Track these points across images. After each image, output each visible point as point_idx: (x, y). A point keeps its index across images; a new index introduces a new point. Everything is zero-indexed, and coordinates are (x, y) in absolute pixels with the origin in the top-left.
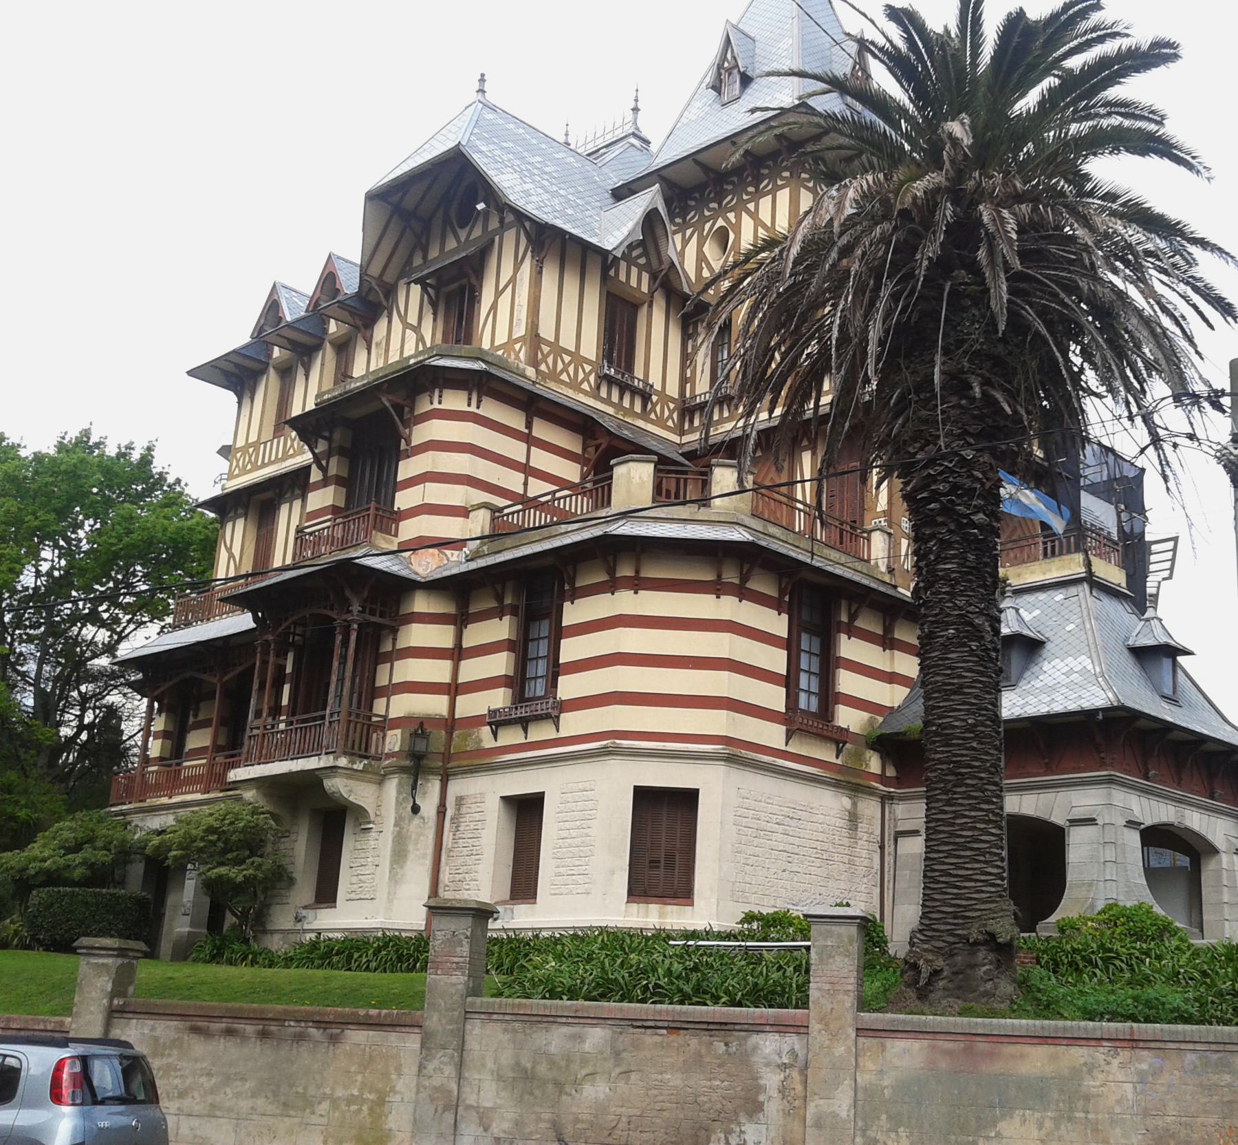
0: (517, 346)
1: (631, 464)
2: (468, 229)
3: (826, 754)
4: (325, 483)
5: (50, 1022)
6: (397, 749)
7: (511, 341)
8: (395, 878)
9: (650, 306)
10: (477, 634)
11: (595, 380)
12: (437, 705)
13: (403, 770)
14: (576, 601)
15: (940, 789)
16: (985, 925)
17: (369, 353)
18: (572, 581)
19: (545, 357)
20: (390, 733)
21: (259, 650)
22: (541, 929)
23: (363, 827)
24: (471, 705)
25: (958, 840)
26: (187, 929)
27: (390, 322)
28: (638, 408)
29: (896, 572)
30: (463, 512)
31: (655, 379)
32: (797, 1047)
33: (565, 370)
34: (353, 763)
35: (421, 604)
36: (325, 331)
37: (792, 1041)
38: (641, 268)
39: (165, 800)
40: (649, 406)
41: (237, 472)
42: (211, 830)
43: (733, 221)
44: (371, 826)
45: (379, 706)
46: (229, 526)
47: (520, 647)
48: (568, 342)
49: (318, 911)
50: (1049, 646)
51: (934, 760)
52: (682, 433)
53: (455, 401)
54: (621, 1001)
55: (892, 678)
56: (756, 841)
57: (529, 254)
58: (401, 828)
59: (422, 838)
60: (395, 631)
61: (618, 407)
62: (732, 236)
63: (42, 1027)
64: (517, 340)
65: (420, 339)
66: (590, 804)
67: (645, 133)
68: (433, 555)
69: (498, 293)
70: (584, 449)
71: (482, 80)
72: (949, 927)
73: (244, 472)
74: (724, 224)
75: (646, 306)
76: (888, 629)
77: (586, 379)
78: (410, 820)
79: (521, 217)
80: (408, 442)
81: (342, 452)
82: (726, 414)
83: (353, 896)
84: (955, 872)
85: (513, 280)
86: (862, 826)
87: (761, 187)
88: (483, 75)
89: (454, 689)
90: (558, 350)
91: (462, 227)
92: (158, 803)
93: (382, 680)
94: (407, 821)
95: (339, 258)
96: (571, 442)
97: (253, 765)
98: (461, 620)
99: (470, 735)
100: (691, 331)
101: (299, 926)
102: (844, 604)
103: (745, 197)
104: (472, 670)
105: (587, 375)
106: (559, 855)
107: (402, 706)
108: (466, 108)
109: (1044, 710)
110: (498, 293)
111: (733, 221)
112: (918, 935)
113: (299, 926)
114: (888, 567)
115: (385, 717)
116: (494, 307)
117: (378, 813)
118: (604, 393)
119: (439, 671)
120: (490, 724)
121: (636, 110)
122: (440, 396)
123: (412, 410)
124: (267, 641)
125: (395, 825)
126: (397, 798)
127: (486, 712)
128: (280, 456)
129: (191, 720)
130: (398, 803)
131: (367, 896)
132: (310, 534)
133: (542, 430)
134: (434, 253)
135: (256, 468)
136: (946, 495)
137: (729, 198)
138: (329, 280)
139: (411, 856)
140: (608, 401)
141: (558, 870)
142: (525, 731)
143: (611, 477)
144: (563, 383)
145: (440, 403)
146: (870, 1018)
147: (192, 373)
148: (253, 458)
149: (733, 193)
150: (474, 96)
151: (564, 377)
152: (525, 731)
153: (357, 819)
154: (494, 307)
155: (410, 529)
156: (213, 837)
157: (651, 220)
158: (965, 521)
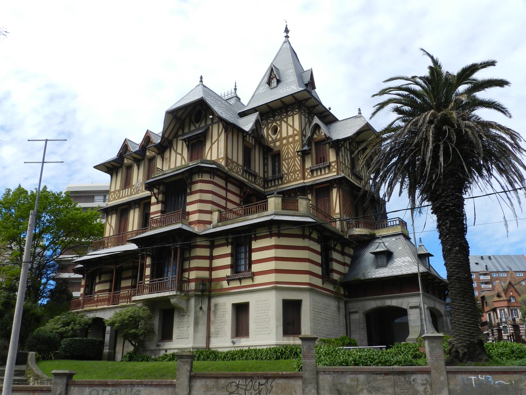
0: (221, 160)
2: (199, 123)
3: (331, 287)
4: (158, 202)
7: (218, 158)
9: (255, 149)
10: (217, 252)
11: (242, 171)
12: (205, 274)
14: (257, 241)
15: (459, 296)
16: (479, 338)
18: (255, 235)
19: (230, 164)
20: (191, 283)
25: (467, 312)
26: (108, 351)
28: (253, 181)
29: (344, 232)
30: (210, 212)
31: (257, 171)
32: (428, 378)
33: (235, 168)
34: (181, 293)
37: (425, 376)
38: (253, 137)
39: (95, 308)
40: (256, 180)
41: (117, 198)
42: (130, 317)
43: (279, 124)
44: (185, 314)
45: (186, 275)
46: (110, 217)
47: (235, 256)
48: (235, 159)
50: (394, 254)
51: (455, 287)
52: (265, 188)
53: (206, 177)
54: (384, 366)
55: (344, 264)
56: (318, 316)
57: (224, 131)
61: (248, 180)
64: (221, 159)
65: (183, 157)
67: (239, 96)
68: (202, 226)
70: (241, 192)
71: (201, 78)
72: (467, 339)
75: (254, 149)
76: (343, 249)
77: (240, 171)
79: (221, 120)
80: (191, 190)
81: (163, 193)
83: (179, 337)
84: (467, 322)
86: (341, 310)
87: (288, 114)
88: (201, 76)
89: (211, 269)
90: (233, 162)
91: (197, 122)
92: (93, 308)
93: (186, 266)
95: (150, 132)
96: (237, 191)
100: (266, 156)
101: (158, 348)
102: (332, 241)
103: (283, 117)
104: (217, 263)
105: (240, 170)
107: (193, 275)
108: (197, 86)
109: (400, 273)
110: (212, 144)
111: (279, 124)
112: (455, 342)
113: (158, 348)
114: (341, 230)
115: (188, 278)
118: (245, 176)
119: (205, 263)
120: (227, 280)
121: (235, 89)
122: (202, 176)
123: (191, 179)
124: (143, 254)
126: (195, 305)
127: (226, 276)
128: (129, 194)
129: (97, 281)
130: (195, 306)
131: (185, 337)
132: (155, 220)
133: (230, 187)
134: (186, 130)
135: (119, 198)
136: (452, 207)
137: (277, 117)
138: (147, 138)
140: (246, 178)
141: (257, 327)
142: (240, 282)
143: (267, 201)
144: (234, 172)
145: (202, 178)
146: (450, 368)
147: (95, 167)
148: (118, 195)
149: (279, 115)
151: (234, 170)
152: (240, 282)
153: (179, 312)
156: (131, 319)
157: (257, 123)
158: (458, 215)
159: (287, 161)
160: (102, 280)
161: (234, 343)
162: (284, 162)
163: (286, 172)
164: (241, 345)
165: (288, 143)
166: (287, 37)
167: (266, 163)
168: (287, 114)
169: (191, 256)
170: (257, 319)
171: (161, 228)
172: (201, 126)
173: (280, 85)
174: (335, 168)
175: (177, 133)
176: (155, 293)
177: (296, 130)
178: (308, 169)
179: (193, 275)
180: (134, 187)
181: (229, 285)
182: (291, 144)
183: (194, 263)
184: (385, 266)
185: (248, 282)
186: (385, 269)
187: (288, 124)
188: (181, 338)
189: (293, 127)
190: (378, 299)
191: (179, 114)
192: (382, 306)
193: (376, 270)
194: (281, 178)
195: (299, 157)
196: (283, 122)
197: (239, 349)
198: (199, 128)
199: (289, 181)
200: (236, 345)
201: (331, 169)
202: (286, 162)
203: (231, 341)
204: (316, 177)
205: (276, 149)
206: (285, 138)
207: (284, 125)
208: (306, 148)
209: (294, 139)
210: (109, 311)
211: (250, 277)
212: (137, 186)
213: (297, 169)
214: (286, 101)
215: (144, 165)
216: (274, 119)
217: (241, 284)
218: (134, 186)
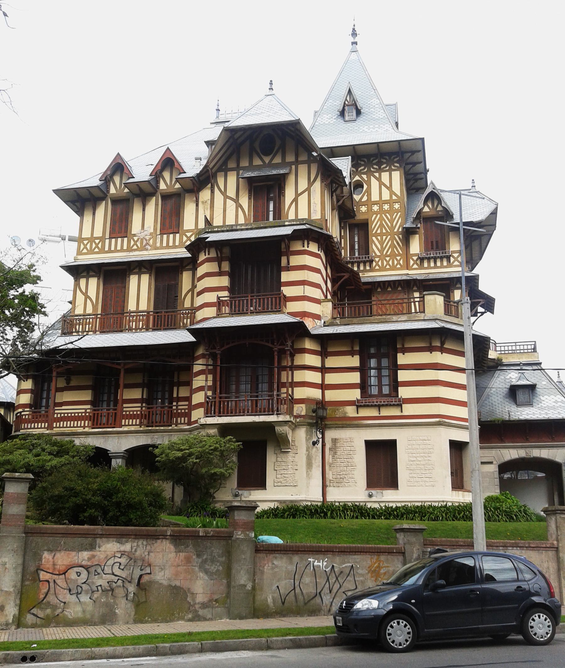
1: (436, 296)
5: (548, 544)
6: (303, 413)
8: (309, 476)
10: (331, 362)
12: (316, 394)
13: (310, 425)
17: (197, 205)
21: (219, 356)
22: (447, 502)
23: (283, 450)
24: (331, 396)
27: (212, 192)
35: (308, 344)
36: (158, 187)
43: (366, 179)
44: (289, 450)
47: (363, 369)
49: (251, 491)
53: (313, 247)
58: (309, 452)
59: (317, 457)
60: (292, 356)
62: (365, 187)
63: (544, 546)
65: (239, 206)
66: (429, 447)
69: (297, 195)
71: (271, 83)
73: (91, 252)
74: (360, 179)
78: (312, 448)
82: (368, 268)
83: (279, 484)
85: (308, 190)
88: (271, 81)
91: (267, 154)
94: (311, 448)
97: (215, 416)
98: (324, 354)
99: (337, 410)
100: (342, 225)
104: (331, 379)
106: (412, 468)
107: (300, 393)
110: (297, 195)
111: (366, 179)
116: (296, 200)
117: (293, 444)
122: (308, 244)
125: (307, 451)
126: (306, 438)
130: (307, 440)
131: (292, 484)
134: (245, 163)
135: (102, 251)
137: (362, 168)
139: (314, 466)
141: (411, 475)
145: (308, 247)
147: (56, 192)
154: (296, 200)
155: (292, 307)
159: (379, 238)
160: (72, 384)
161: (370, 496)
162: (374, 238)
163: (378, 254)
164: (385, 498)
165: (381, 211)
167: (343, 234)
169: (295, 364)
170: (411, 465)
171: (238, 316)
172: (273, 162)
173: (362, 118)
174: (458, 261)
175: (225, 163)
176: (243, 415)
177: (396, 195)
178: (415, 255)
179: (300, 393)
180: (136, 238)
181: (358, 413)
182: (387, 214)
183: (299, 376)
184: (529, 404)
185: (395, 412)
186: (531, 408)
187: (381, 184)
188: (282, 485)
189: (390, 188)
190: (522, 447)
191: (236, 136)
192: (526, 456)
193: (519, 409)
194: (371, 262)
195: (401, 236)
197: (403, 504)
198: (277, 166)
199: (383, 269)
200: (374, 499)
201: (452, 261)
202: (377, 239)
203: (367, 492)
204: (426, 268)
205: (360, 217)
206: (375, 203)
207: (374, 183)
208: (408, 225)
209: (391, 207)
210: (117, 438)
211: (398, 405)
212: (142, 237)
213: (397, 253)
214: (384, 148)
215: (157, 205)
216: (357, 170)
217: (380, 414)
218: (135, 235)
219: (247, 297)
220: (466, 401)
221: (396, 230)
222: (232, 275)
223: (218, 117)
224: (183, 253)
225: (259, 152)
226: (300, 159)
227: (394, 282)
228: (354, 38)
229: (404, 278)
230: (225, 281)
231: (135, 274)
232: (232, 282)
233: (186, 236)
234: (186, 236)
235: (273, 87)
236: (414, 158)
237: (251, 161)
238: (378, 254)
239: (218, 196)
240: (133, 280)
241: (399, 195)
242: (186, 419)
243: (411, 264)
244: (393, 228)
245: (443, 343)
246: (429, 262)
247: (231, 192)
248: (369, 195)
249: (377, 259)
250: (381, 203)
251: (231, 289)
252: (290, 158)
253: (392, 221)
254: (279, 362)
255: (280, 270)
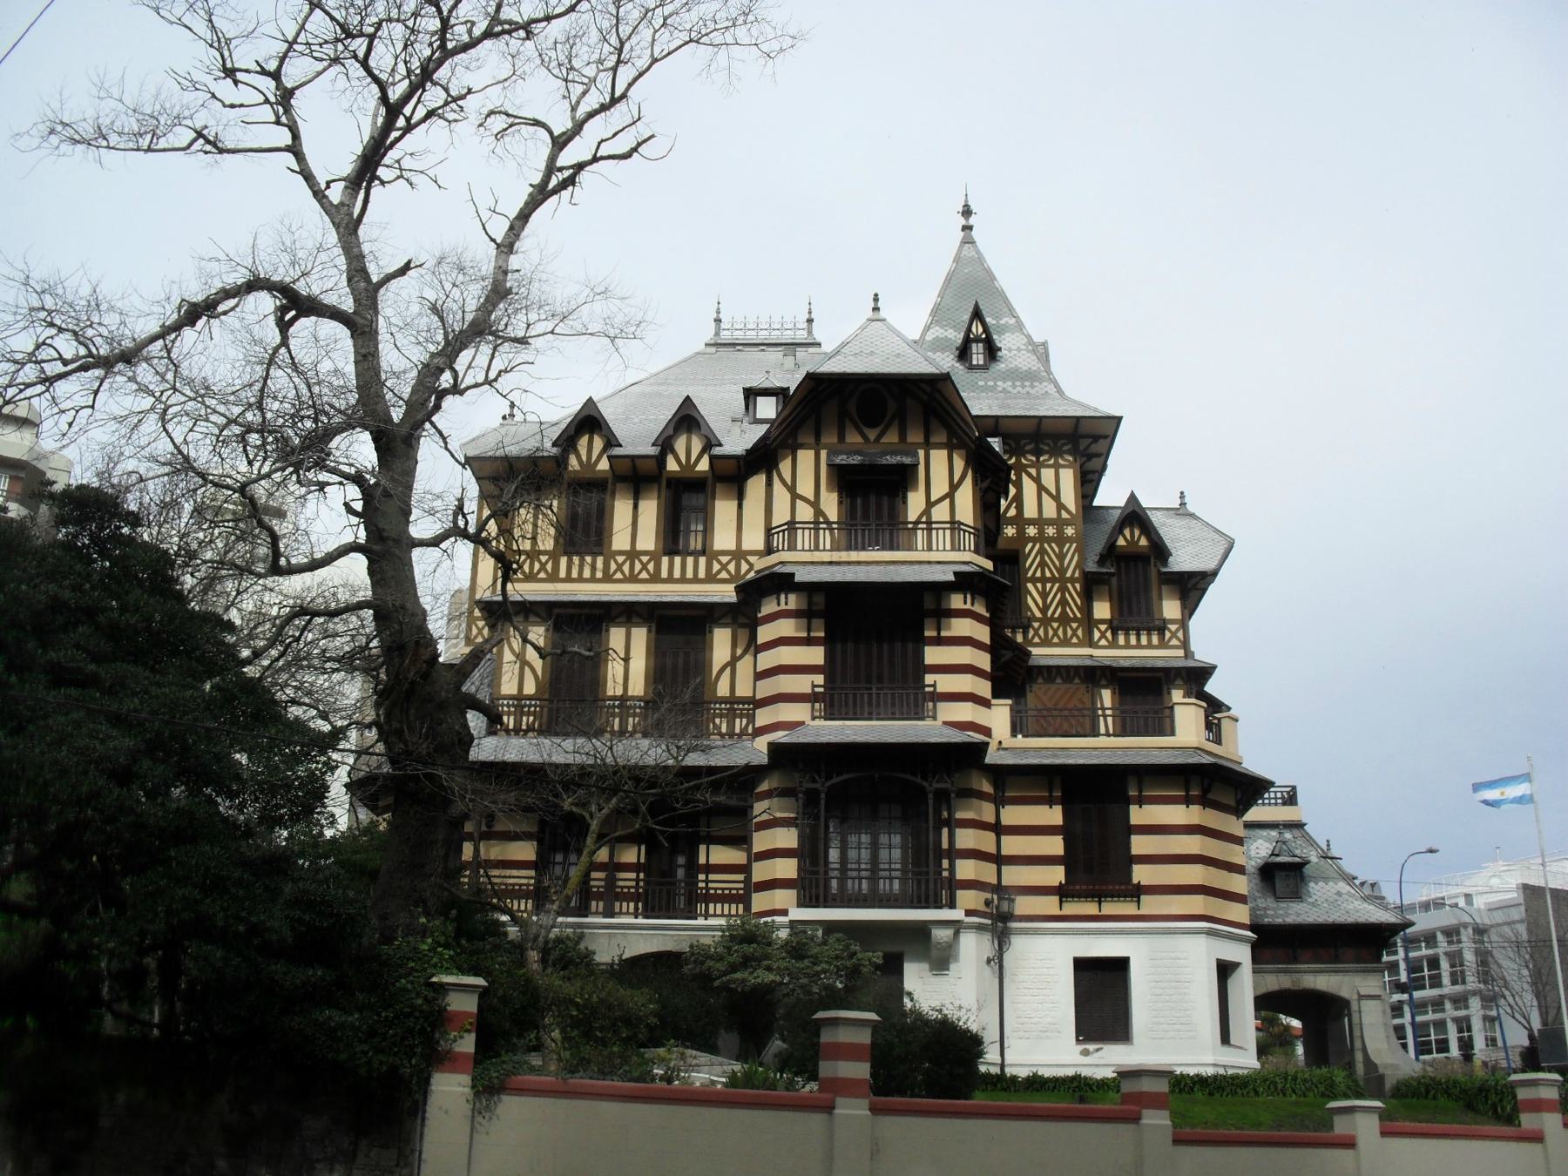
27: (769, 484)
88: (876, 295)
91: (872, 425)
121: (810, 321)
134: (830, 438)
145: (972, 604)
150: (870, 314)
162: (1030, 586)
163: (1038, 614)
165: (1041, 538)
166: (967, 228)
168: (1038, 459)
182: (1053, 545)
185: (1128, 908)
190: (1285, 971)
195: (1078, 586)
196: (1025, 478)
206: (1031, 522)
208: (1092, 567)
213: (1072, 616)
219: (871, 689)
220: (1246, 893)
221: (1068, 575)
222: (828, 642)
223: (717, 334)
224: (725, 593)
225: (855, 416)
226: (933, 439)
227: (1068, 668)
228: (967, 219)
229: (1088, 662)
230: (816, 655)
231: (619, 625)
232: (829, 656)
233: (719, 562)
234: (719, 562)
235: (880, 305)
236: (1095, 448)
237: (841, 438)
238: (1038, 614)
239: (781, 495)
240: (616, 637)
241: (1074, 512)
242: (741, 906)
243: (1096, 639)
244: (1062, 570)
245: (1205, 791)
246: (1127, 635)
247: (806, 487)
248: (1020, 508)
249: (1036, 625)
250: (1040, 522)
251: (828, 669)
252: (915, 437)
253: (1061, 557)
254: (938, 812)
255: (924, 641)
